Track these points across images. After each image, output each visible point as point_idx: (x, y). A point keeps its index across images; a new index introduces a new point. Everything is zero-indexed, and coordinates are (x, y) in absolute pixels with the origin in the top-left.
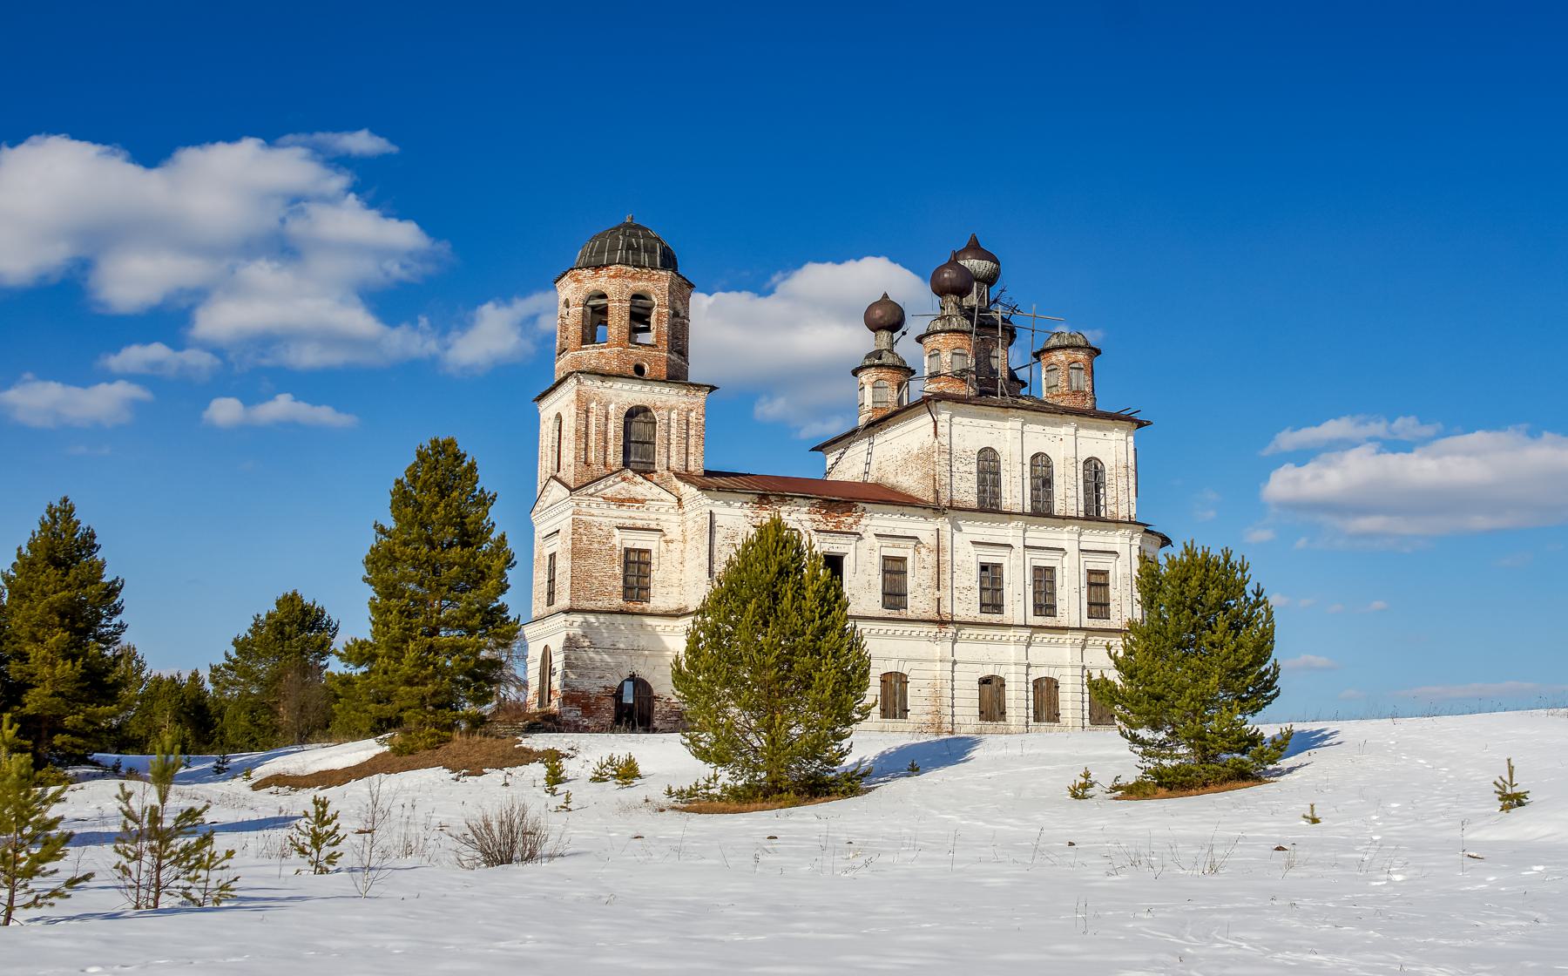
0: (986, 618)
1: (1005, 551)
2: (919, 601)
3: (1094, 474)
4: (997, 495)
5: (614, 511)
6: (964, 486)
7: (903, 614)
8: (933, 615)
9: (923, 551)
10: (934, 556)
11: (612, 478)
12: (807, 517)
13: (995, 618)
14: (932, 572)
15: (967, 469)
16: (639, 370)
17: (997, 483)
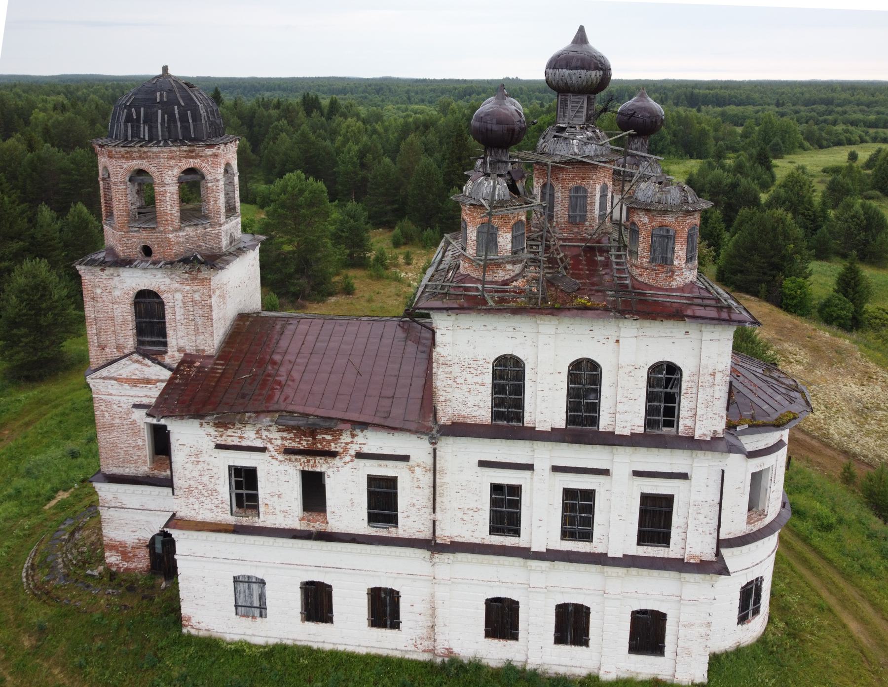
1: (526, 474)
2: (411, 520)
3: (665, 382)
4: (519, 405)
6: (473, 399)
7: (393, 532)
8: (426, 534)
9: (418, 470)
10: (431, 475)
11: (123, 361)
12: (277, 435)
13: (509, 541)
14: (428, 492)
15: (478, 380)
16: (147, 251)
17: (519, 390)
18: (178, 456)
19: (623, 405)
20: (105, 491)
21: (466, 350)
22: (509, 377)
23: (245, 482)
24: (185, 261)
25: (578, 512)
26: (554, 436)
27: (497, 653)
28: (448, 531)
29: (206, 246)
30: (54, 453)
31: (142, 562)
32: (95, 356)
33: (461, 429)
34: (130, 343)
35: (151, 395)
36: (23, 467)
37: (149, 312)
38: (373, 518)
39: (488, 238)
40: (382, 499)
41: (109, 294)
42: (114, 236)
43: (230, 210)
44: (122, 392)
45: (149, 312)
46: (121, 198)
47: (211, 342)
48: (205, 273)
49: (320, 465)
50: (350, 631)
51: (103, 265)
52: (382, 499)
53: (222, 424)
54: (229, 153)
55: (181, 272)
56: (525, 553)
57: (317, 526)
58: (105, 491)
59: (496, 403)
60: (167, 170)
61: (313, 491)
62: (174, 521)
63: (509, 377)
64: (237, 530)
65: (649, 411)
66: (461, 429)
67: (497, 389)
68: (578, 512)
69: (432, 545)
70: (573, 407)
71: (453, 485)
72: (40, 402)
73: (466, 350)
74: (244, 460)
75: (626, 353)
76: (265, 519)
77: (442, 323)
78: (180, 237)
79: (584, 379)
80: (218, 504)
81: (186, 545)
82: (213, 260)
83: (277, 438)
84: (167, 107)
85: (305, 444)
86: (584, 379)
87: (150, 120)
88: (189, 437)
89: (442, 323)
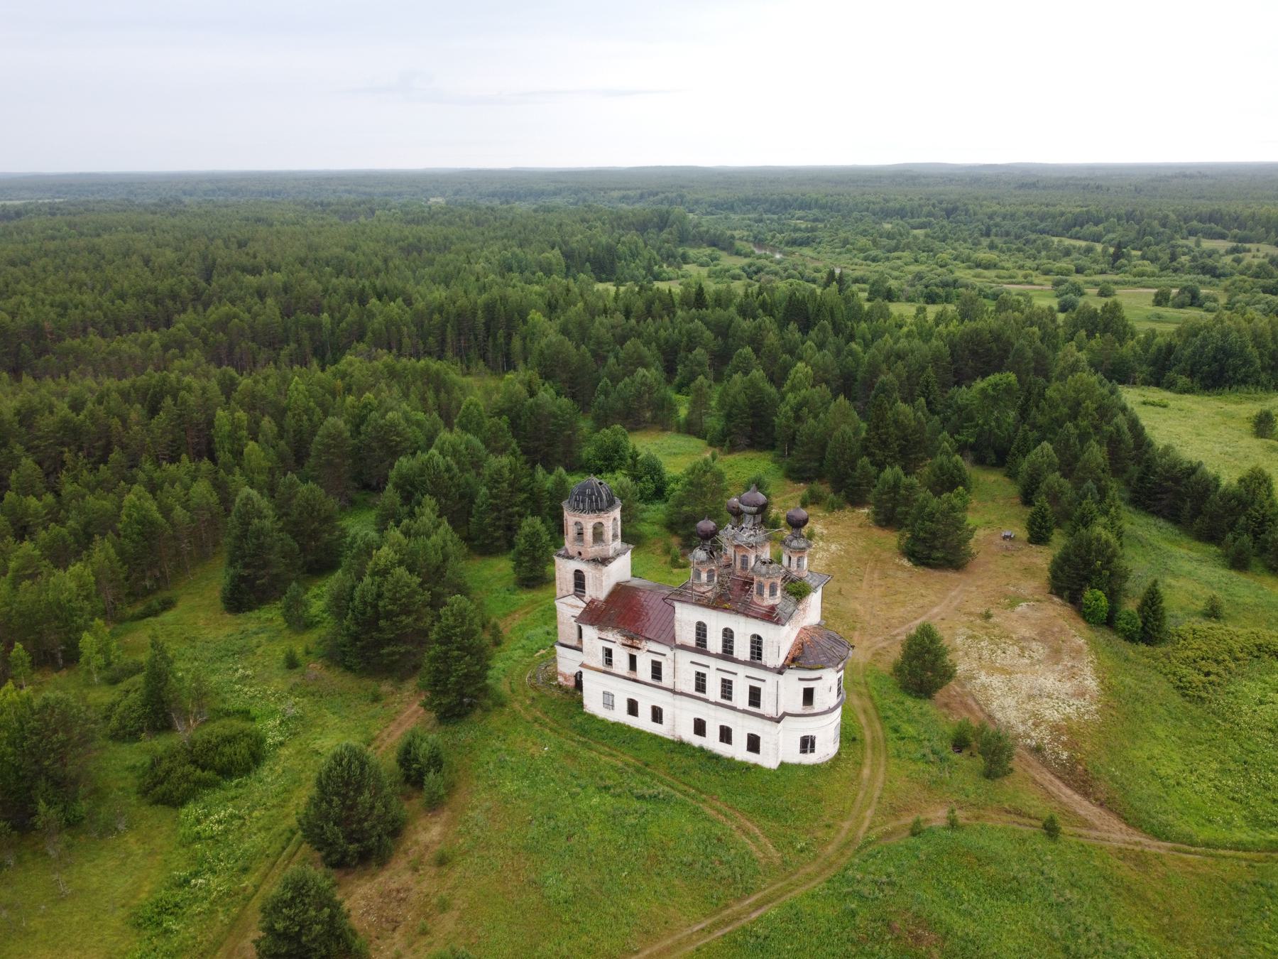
0: (698, 694)
2: (666, 680)
5: (570, 609)
13: (701, 695)
16: (580, 554)
17: (705, 636)
18: (585, 639)
19: (742, 649)
20: (559, 649)
21: (686, 617)
22: (701, 630)
23: (609, 653)
24: (594, 560)
25: (727, 688)
26: (717, 656)
27: (697, 741)
28: (679, 688)
29: (603, 554)
30: (540, 631)
31: (572, 683)
32: (559, 595)
33: (683, 647)
34: (572, 589)
35: (578, 612)
36: (526, 635)
37: (579, 579)
38: (653, 677)
39: (698, 575)
40: (657, 670)
41: (564, 570)
42: (569, 544)
43: (615, 536)
44: (568, 608)
45: (579, 579)
46: (571, 531)
47: (602, 594)
48: (600, 567)
49: (634, 652)
50: (643, 722)
51: (563, 557)
52: (657, 670)
53: (601, 630)
54: (617, 513)
55: (592, 565)
56: (706, 701)
57: (633, 676)
58: (559, 649)
59: (698, 639)
60: (589, 522)
61: (633, 659)
62: (582, 665)
63: (701, 630)
64: (605, 672)
65: (752, 653)
66: (683, 647)
67: (698, 634)
68: (727, 688)
69: (673, 692)
70: (724, 646)
71: (681, 669)
72: (533, 602)
73: (686, 617)
74: (609, 645)
75: (744, 629)
76: (614, 670)
77: (677, 605)
78: (592, 550)
79: (728, 636)
80: (599, 661)
81: (587, 678)
82: (604, 561)
83: (620, 639)
84: (590, 496)
85: (629, 643)
86: (728, 636)
87: (583, 501)
88: (590, 632)
89: (677, 605)
